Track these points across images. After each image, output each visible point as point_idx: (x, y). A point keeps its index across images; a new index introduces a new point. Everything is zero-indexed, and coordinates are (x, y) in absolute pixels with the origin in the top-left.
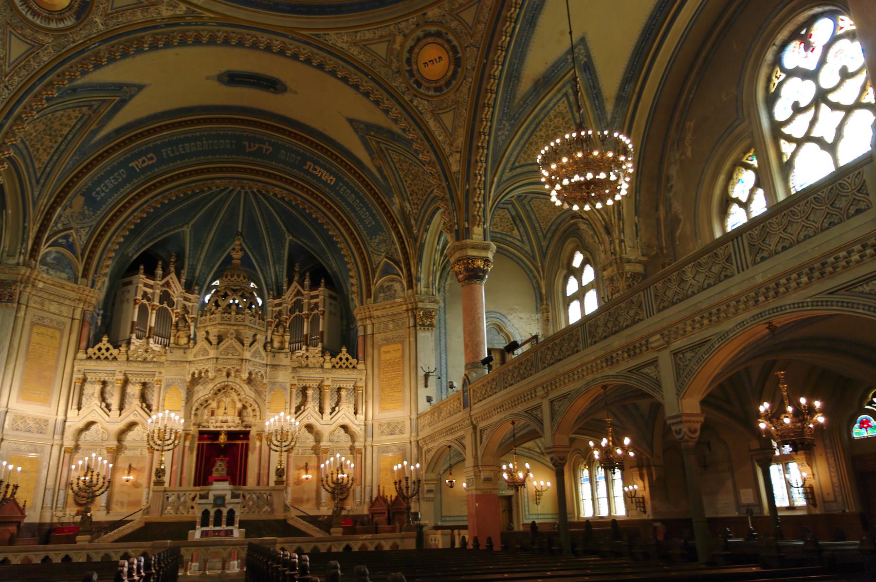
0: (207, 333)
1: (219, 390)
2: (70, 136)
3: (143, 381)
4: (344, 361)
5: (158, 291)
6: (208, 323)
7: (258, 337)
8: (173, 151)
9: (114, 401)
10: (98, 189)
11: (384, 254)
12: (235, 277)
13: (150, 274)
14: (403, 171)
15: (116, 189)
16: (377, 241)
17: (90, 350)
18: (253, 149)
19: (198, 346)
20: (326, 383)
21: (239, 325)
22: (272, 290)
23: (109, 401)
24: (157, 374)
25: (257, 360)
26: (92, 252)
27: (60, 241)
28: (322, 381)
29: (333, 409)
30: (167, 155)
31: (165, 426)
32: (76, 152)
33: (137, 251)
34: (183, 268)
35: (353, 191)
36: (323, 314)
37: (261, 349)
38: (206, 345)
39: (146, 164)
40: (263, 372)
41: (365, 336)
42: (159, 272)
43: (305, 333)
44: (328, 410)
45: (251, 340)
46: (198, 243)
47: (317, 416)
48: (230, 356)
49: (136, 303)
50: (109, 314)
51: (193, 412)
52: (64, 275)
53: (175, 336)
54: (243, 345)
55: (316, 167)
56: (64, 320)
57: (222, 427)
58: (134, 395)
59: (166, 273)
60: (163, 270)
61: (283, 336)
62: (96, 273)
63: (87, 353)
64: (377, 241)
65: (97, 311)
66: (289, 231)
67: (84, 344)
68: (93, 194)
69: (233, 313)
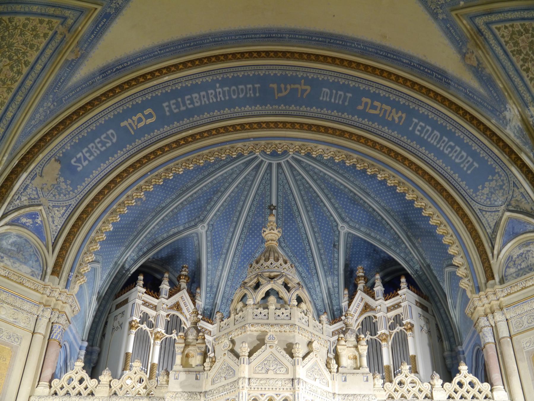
0: (233, 342)
2: (39, 67)
4: (467, 387)
6: (232, 327)
7: (315, 345)
8: (178, 106)
10: (80, 155)
11: (503, 207)
12: (272, 260)
14: (519, 52)
15: (103, 157)
16: (486, 191)
17: (55, 382)
18: (284, 94)
19: (217, 365)
25: (317, 383)
26: (68, 241)
27: (24, 220)
30: (170, 110)
32: (47, 94)
33: (136, 262)
34: (199, 286)
35: (435, 126)
38: (230, 359)
39: (141, 124)
41: (498, 342)
45: (305, 350)
46: (218, 252)
48: (271, 375)
49: (131, 327)
50: (97, 348)
52: (25, 269)
54: (292, 356)
55: (376, 103)
56: (20, 332)
59: (174, 290)
60: (171, 283)
61: (356, 347)
62: (71, 270)
63: (51, 387)
64: (486, 191)
66: (343, 220)
67: (48, 373)
68: (73, 161)
69: (272, 307)
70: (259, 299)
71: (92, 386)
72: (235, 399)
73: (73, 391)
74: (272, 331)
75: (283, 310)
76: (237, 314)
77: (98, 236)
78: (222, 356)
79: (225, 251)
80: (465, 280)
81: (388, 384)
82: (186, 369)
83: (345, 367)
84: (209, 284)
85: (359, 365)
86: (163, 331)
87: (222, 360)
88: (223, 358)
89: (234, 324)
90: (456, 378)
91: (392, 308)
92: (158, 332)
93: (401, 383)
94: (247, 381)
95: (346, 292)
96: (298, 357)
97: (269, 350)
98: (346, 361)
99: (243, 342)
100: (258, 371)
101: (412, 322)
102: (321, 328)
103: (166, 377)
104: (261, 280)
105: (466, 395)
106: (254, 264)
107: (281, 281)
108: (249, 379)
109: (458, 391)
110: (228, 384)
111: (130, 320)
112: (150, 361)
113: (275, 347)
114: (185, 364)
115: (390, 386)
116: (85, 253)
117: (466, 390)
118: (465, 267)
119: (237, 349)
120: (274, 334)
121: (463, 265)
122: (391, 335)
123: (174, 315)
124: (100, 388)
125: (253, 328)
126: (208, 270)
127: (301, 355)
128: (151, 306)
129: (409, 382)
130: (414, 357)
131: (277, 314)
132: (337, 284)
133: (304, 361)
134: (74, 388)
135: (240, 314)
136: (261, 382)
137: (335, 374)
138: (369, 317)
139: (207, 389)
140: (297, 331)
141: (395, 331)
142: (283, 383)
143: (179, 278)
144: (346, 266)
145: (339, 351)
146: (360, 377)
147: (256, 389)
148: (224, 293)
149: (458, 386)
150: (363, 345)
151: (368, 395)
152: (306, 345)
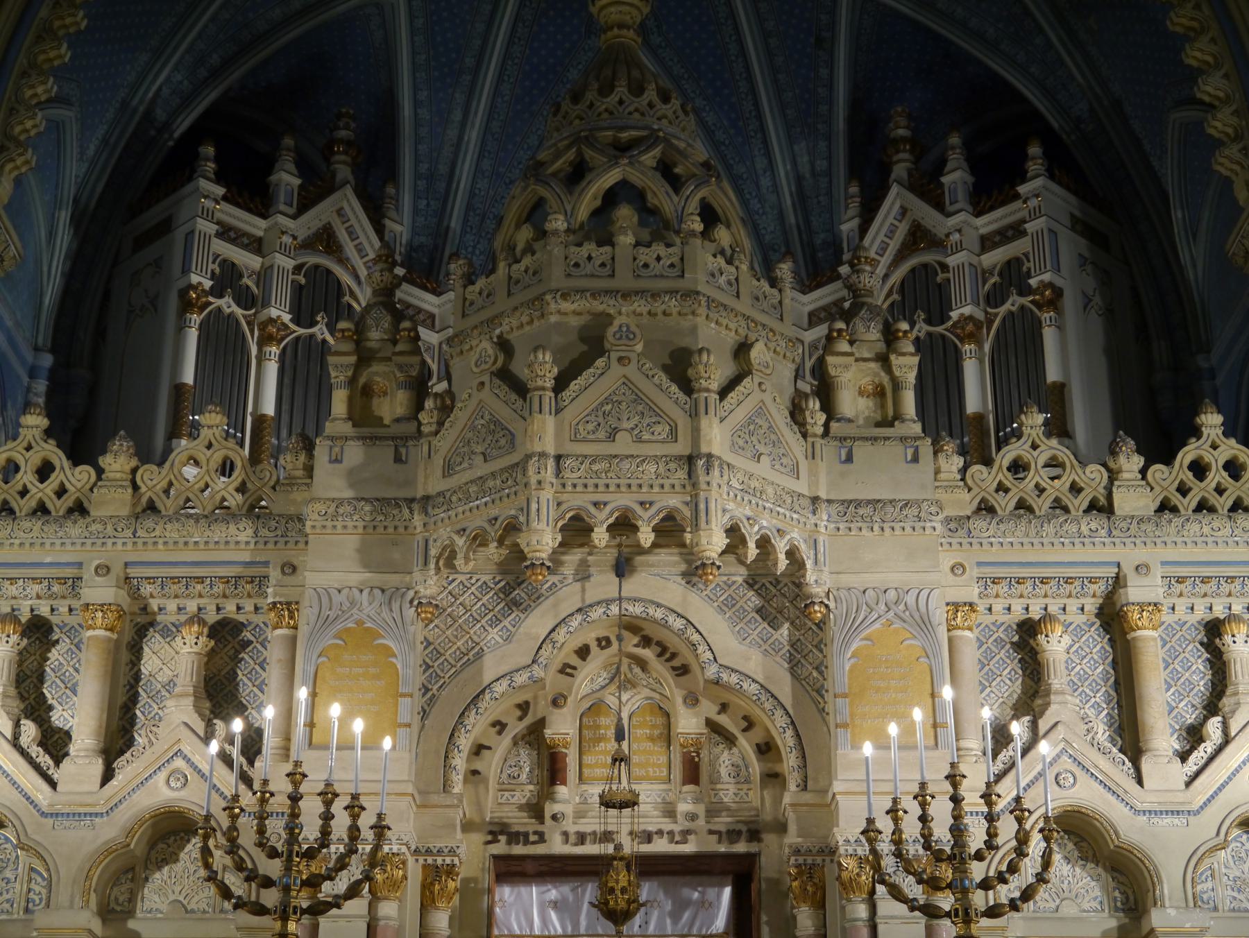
0: (504, 346)
1: (583, 652)
3: (212, 617)
4: (1217, 476)
5: (285, 262)
7: (758, 353)
9: (81, 715)
12: (621, 90)
13: (251, 190)
19: (460, 416)
20: (1136, 591)
21: (655, 295)
22: (789, 253)
23: (58, 718)
24: (274, 574)
25: (763, 468)
28: (1118, 581)
29: (1194, 735)
31: (296, 777)
34: (392, 175)
36: (1054, 299)
37: (780, 417)
38: (497, 402)
40: (796, 535)
42: (287, 179)
43: (972, 404)
44: (1162, 738)
47: (1117, 769)
48: (623, 444)
49: (187, 306)
51: (460, 762)
53: (352, 382)
54: (687, 387)
57: (607, 837)
58: (170, 685)
60: (304, 167)
65: (29, 357)
70: (583, 213)
71: (79, 485)
72: (516, 517)
73: (22, 502)
74: (625, 314)
75: (659, 249)
76: (518, 261)
77: (62, 18)
78: (475, 392)
79: (469, 61)
80: (1233, 150)
81: (977, 469)
82: (366, 431)
83: (850, 421)
84: (424, 168)
85: (891, 413)
86: (286, 318)
87: (473, 403)
88: (478, 398)
89: (509, 294)
90: (1186, 449)
91: (997, 239)
92: (272, 321)
93: (1018, 467)
94: (551, 463)
95: (854, 189)
96: (708, 390)
97: (617, 370)
98: (852, 403)
99: (536, 349)
100: (584, 434)
101: (1059, 282)
102: (776, 301)
103: (302, 458)
104: (589, 153)
105: (1214, 499)
106: (566, 105)
107: (650, 158)
108: (558, 458)
109: (1190, 489)
110: (493, 474)
111: (181, 284)
112: (250, 409)
113: (634, 361)
114: (361, 416)
115: (985, 475)
116: (24, 74)
117: (1213, 485)
118: (1234, 107)
119: (520, 369)
120: (632, 322)
121: (1227, 101)
122: (990, 323)
123: (316, 267)
124: (103, 491)
125: (566, 306)
126: (417, 124)
127: (715, 386)
128: (246, 241)
129: (1041, 461)
130: (1060, 389)
131: (643, 259)
132: (825, 163)
133: (725, 403)
134: (24, 492)
135: (527, 260)
136: (595, 467)
137: (819, 442)
138: (925, 266)
139: (432, 489)
140: (702, 311)
141: (1002, 310)
142: (662, 470)
143: (327, 153)
144: (855, 105)
145: (832, 372)
146: (898, 449)
147: (579, 489)
148: (472, 194)
149: (1190, 474)
150: (904, 354)
151: (918, 503)
152: (728, 356)
